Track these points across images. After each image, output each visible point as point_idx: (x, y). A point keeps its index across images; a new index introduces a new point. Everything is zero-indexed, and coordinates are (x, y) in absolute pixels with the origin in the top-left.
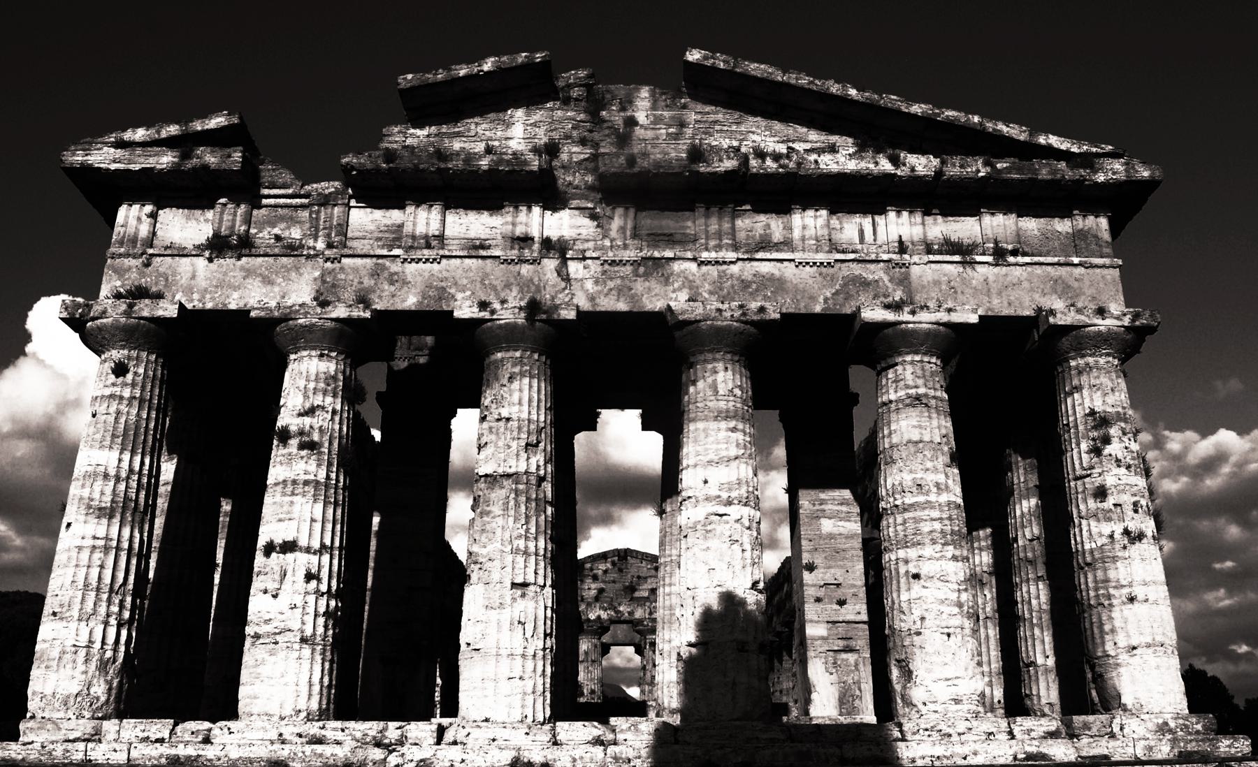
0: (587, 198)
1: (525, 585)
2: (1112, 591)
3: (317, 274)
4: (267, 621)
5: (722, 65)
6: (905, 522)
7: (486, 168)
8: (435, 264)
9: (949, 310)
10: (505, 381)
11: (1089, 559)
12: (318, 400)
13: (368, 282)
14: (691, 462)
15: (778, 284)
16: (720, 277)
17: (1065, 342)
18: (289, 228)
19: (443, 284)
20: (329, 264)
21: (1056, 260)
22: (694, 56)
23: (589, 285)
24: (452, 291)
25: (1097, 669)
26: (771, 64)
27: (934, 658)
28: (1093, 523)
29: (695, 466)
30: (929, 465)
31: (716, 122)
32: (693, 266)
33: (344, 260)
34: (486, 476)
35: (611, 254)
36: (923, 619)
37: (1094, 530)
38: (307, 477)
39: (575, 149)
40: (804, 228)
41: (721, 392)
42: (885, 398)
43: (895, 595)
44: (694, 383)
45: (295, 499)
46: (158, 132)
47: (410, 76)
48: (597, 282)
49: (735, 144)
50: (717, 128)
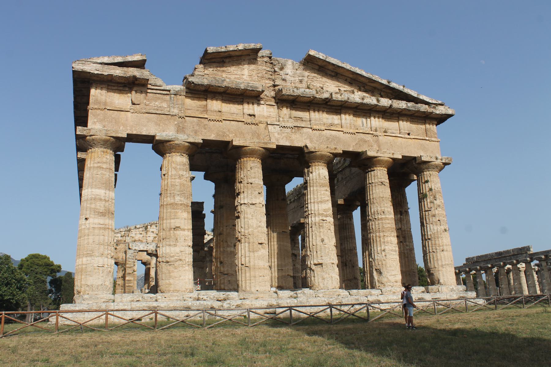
0: (271, 101)
1: (261, 244)
2: (437, 248)
4: (172, 257)
5: (321, 58)
6: (379, 224)
7: (243, 88)
8: (220, 123)
9: (393, 154)
10: (249, 169)
11: (429, 237)
12: (181, 173)
13: (197, 128)
15: (338, 140)
16: (319, 135)
17: (424, 166)
18: (162, 102)
19: (224, 130)
21: (421, 138)
22: (312, 53)
23: (276, 135)
24: (228, 133)
25: (431, 272)
26: (338, 59)
27: (389, 269)
28: (431, 225)
29: (314, 202)
30: (386, 205)
32: (310, 130)
33: (187, 118)
34: (245, 204)
35: (283, 124)
37: (432, 228)
38: (181, 202)
39: (267, 82)
40: (346, 119)
41: (322, 177)
43: (375, 248)
44: (312, 173)
45: (177, 211)
46: (114, 59)
47: (212, 48)
48: (278, 134)
49: (322, 86)
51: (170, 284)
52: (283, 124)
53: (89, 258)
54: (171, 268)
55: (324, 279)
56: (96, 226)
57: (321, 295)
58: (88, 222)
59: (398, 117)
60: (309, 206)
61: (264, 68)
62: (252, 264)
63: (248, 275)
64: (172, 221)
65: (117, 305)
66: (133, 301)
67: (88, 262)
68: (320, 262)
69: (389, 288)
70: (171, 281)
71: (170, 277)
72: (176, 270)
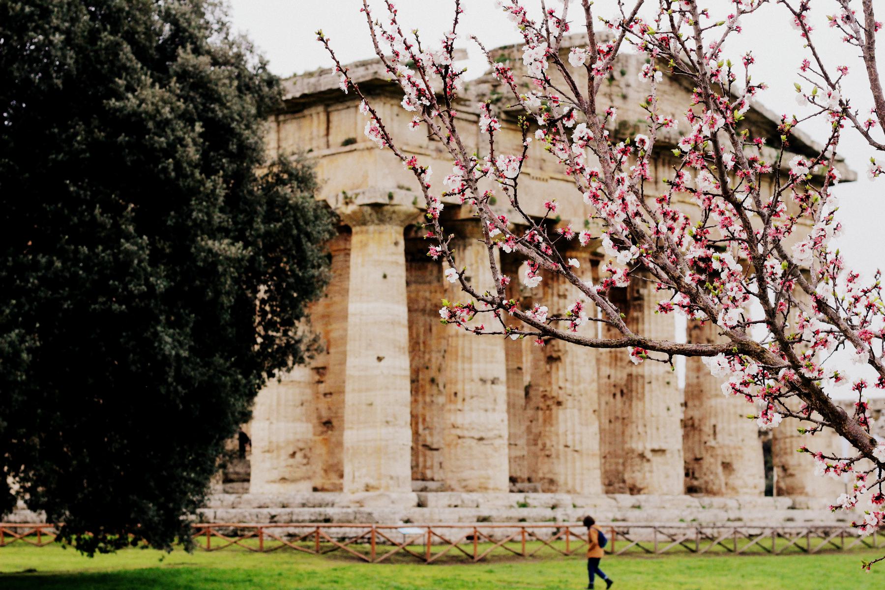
31: (665, 92)
50: (666, 96)
54: (489, 450)
55: (667, 477)
57: (667, 505)
63: (578, 464)
66: (450, 506)
69: (747, 498)
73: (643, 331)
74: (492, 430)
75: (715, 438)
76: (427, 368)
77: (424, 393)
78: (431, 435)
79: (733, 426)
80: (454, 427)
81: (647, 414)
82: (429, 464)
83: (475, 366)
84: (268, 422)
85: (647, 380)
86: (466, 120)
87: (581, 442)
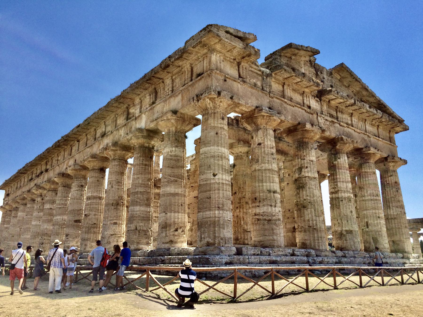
3: (268, 101)
10: (310, 149)
11: (395, 216)
14: (341, 180)
19: (296, 115)
20: (270, 98)
36: (381, 228)
42: (366, 170)
45: (274, 176)
51: (275, 240)
52: (326, 118)
53: (221, 212)
56: (224, 182)
58: (216, 177)
59: (378, 126)
60: (339, 184)
61: (312, 70)
62: (318, 226)
63: (316, 235)
64: (272, 184)
65: (250, 258)
67: (221, 215)
68: (351, 229)
70: (275, 237)
71: (273, 233)
72: (278, 228)
73: (337, 178)
74: (275, 216)
75: (368, 228)
76: (244, 198)
77: (243, 208)
78: (247, 225)
79: (376, 222)
80: (255, 215)
81: (342, 214)
82: (246, 238)
83: (264, 184)
84: (164, 213)
85: (340, 200)
86: (257, 73)
87: (316, 225)
